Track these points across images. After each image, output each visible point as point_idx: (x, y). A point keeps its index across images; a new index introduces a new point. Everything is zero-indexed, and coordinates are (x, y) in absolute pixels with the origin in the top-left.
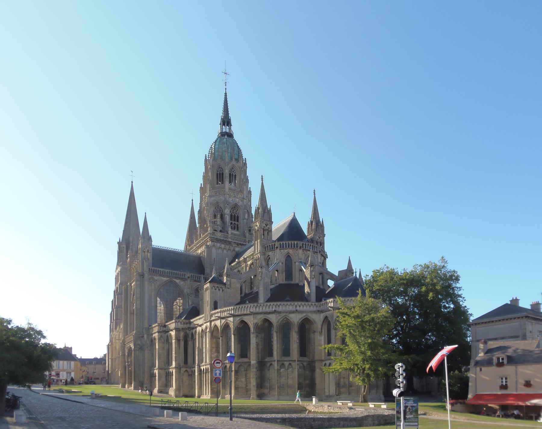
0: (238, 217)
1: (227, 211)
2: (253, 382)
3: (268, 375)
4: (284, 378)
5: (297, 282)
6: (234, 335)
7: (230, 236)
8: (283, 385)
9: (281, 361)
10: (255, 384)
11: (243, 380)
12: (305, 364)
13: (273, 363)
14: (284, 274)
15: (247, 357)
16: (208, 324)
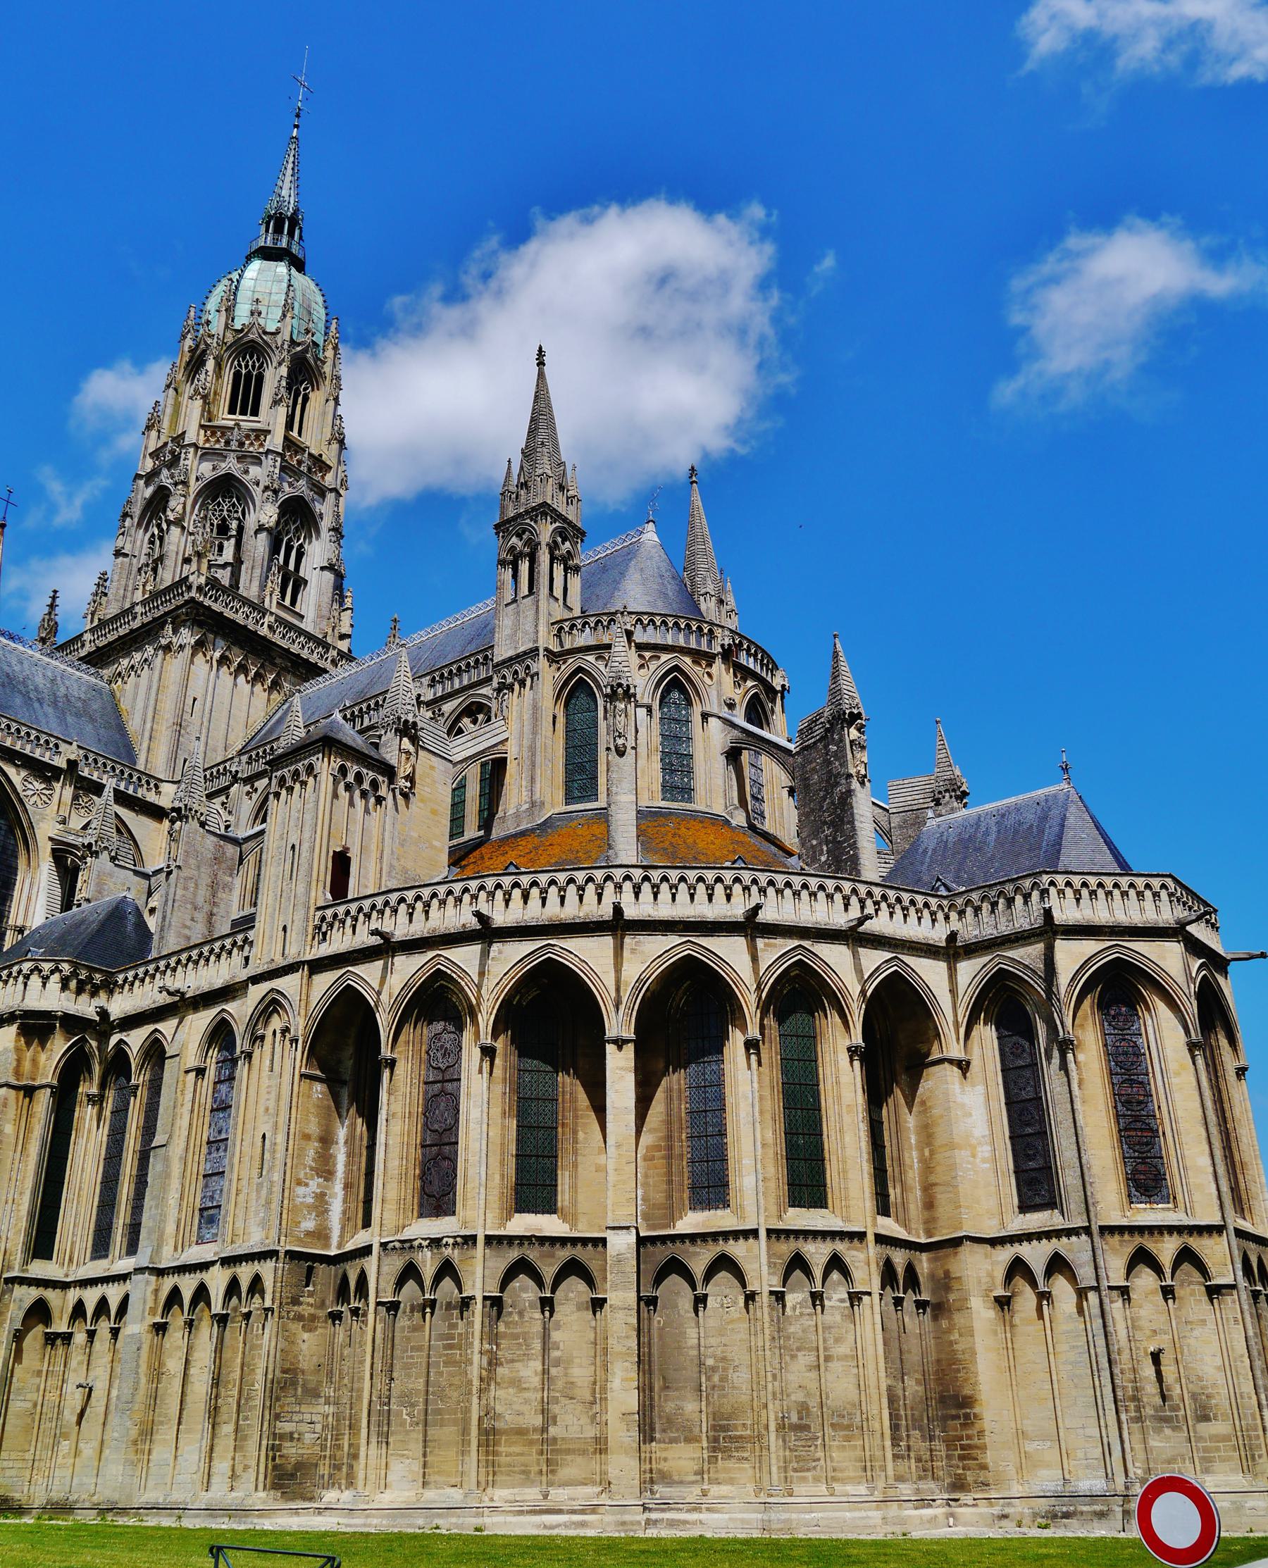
0: (300, 555)
1: (267, 513)
2: (623, 1394)
3: (692, 1333)
4: (805, 1359)
5: (718, 809)
6: (488, 1052)
7: (269, 619)
8: (803, 1409)
9: (788, 1233)
10: (631, 1401)
11: (530, 1371)
12: (899, 1258)
13: (737, 1249)
14: (657, 765)
15: (548, 1206)
16: (289, 985)
